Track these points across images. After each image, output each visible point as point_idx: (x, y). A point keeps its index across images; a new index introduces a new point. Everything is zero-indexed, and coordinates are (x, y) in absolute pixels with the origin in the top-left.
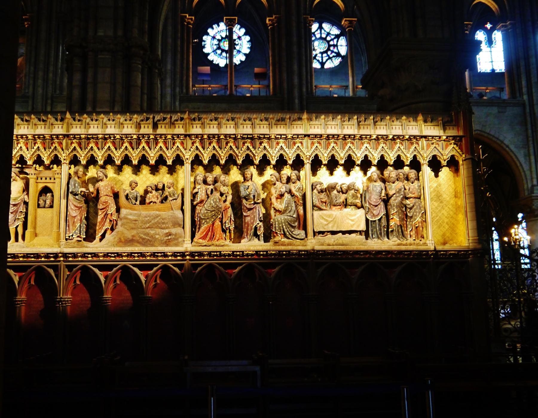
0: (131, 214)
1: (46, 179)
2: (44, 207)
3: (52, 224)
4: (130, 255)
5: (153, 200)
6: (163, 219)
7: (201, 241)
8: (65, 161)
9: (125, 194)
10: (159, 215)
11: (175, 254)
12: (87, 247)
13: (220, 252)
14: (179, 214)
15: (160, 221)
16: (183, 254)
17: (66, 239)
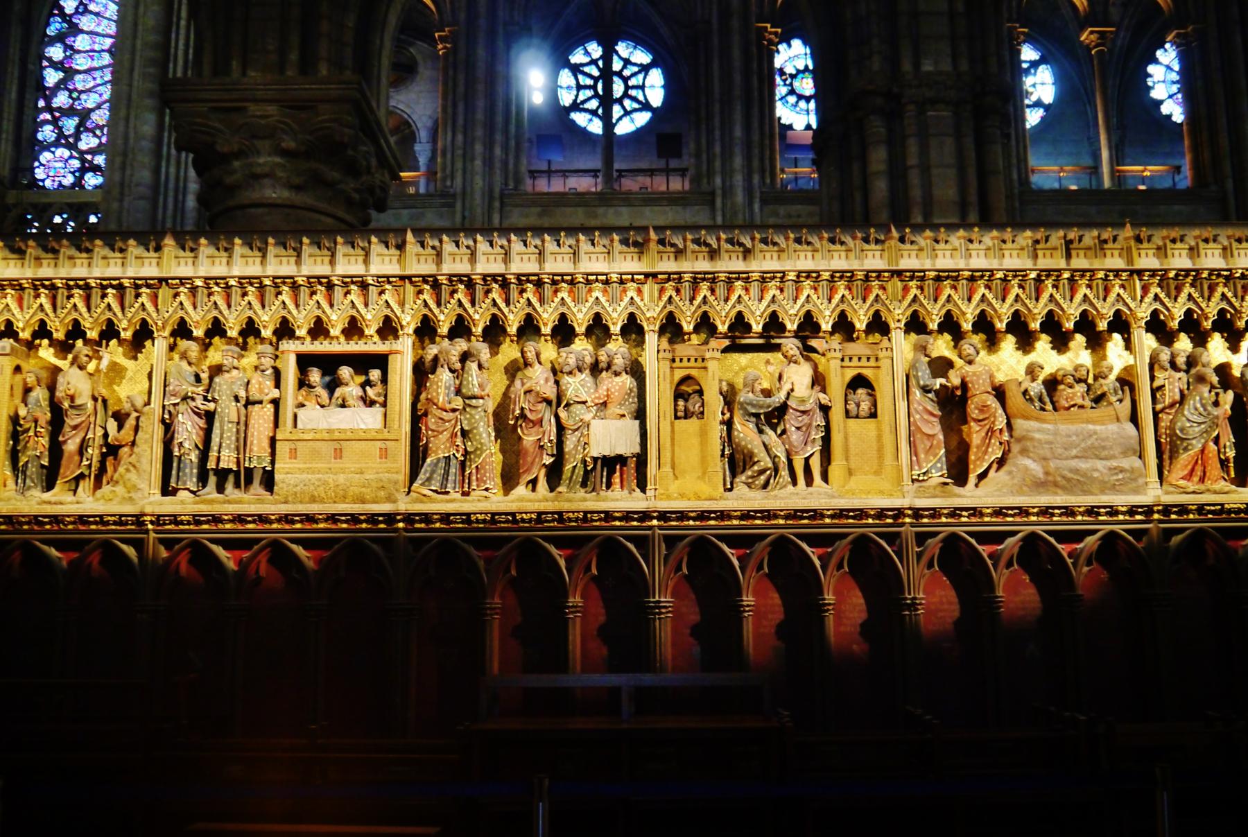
0: (1039, 431)
1: (860, 359)
2: (857, 417)
3: (880, 449)
4: (1045, 511)
5: (1080, 402)
6: (1103, 440)
7: (1182, 483)
8: (898, 325)
9: (1022, 389)
10: (1095, 433)
11: (1132, 510)
12: (959, 496)
13: (1222, 505)
14: (1130, 428)
15: (1096, 444)
16: (1149, 510)
17: (913, 481)
